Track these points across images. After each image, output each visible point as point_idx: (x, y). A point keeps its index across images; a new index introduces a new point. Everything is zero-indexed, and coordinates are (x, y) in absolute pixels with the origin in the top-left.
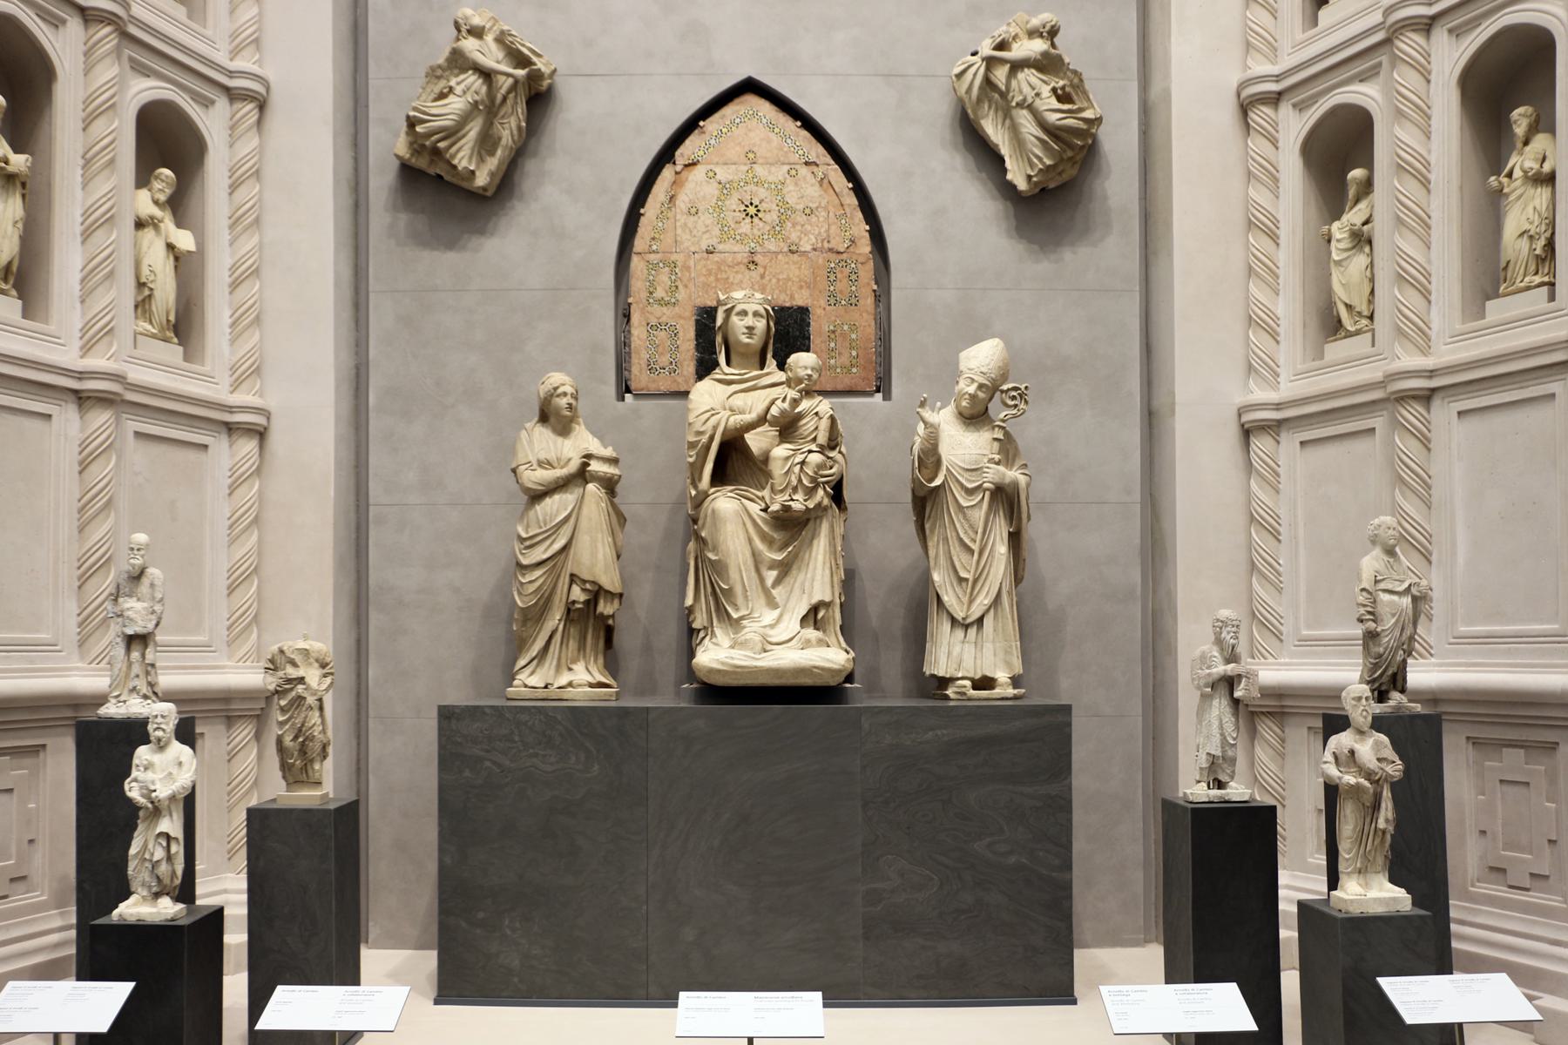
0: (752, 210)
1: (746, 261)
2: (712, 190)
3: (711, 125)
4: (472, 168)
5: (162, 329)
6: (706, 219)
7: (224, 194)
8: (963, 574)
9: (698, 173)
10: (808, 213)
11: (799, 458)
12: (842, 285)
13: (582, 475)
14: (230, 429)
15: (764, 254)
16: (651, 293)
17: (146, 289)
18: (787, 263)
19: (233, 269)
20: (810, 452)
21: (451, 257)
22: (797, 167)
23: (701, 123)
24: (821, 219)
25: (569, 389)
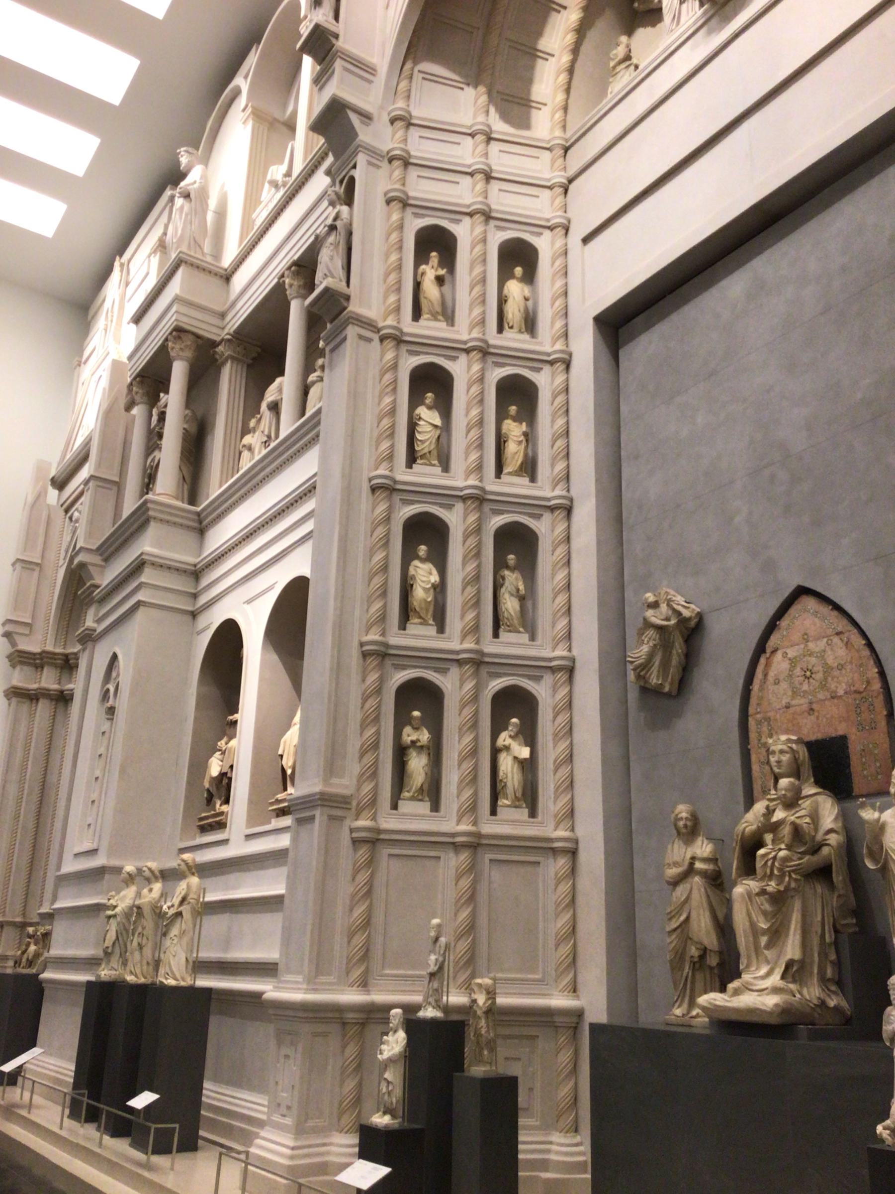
0: (808, 673)
1: (807, 709)
2: (785, 665)
3: (784, 623)
4: (660, 682)
5: (513, 801)
6: (784, 685)
7: (549, 724)
9: (779, 655)
10: (841, 667)
11: (773, 854)
12: (865, 715)
13: (690, 871)
14: (554, 851)
15: (817, 702)
16: (759, 740)
18: (831, 706)
19: (555, 761)
20: (780, 850)
22: (832, 638)
24: (848, 670)
25: (684, 815)
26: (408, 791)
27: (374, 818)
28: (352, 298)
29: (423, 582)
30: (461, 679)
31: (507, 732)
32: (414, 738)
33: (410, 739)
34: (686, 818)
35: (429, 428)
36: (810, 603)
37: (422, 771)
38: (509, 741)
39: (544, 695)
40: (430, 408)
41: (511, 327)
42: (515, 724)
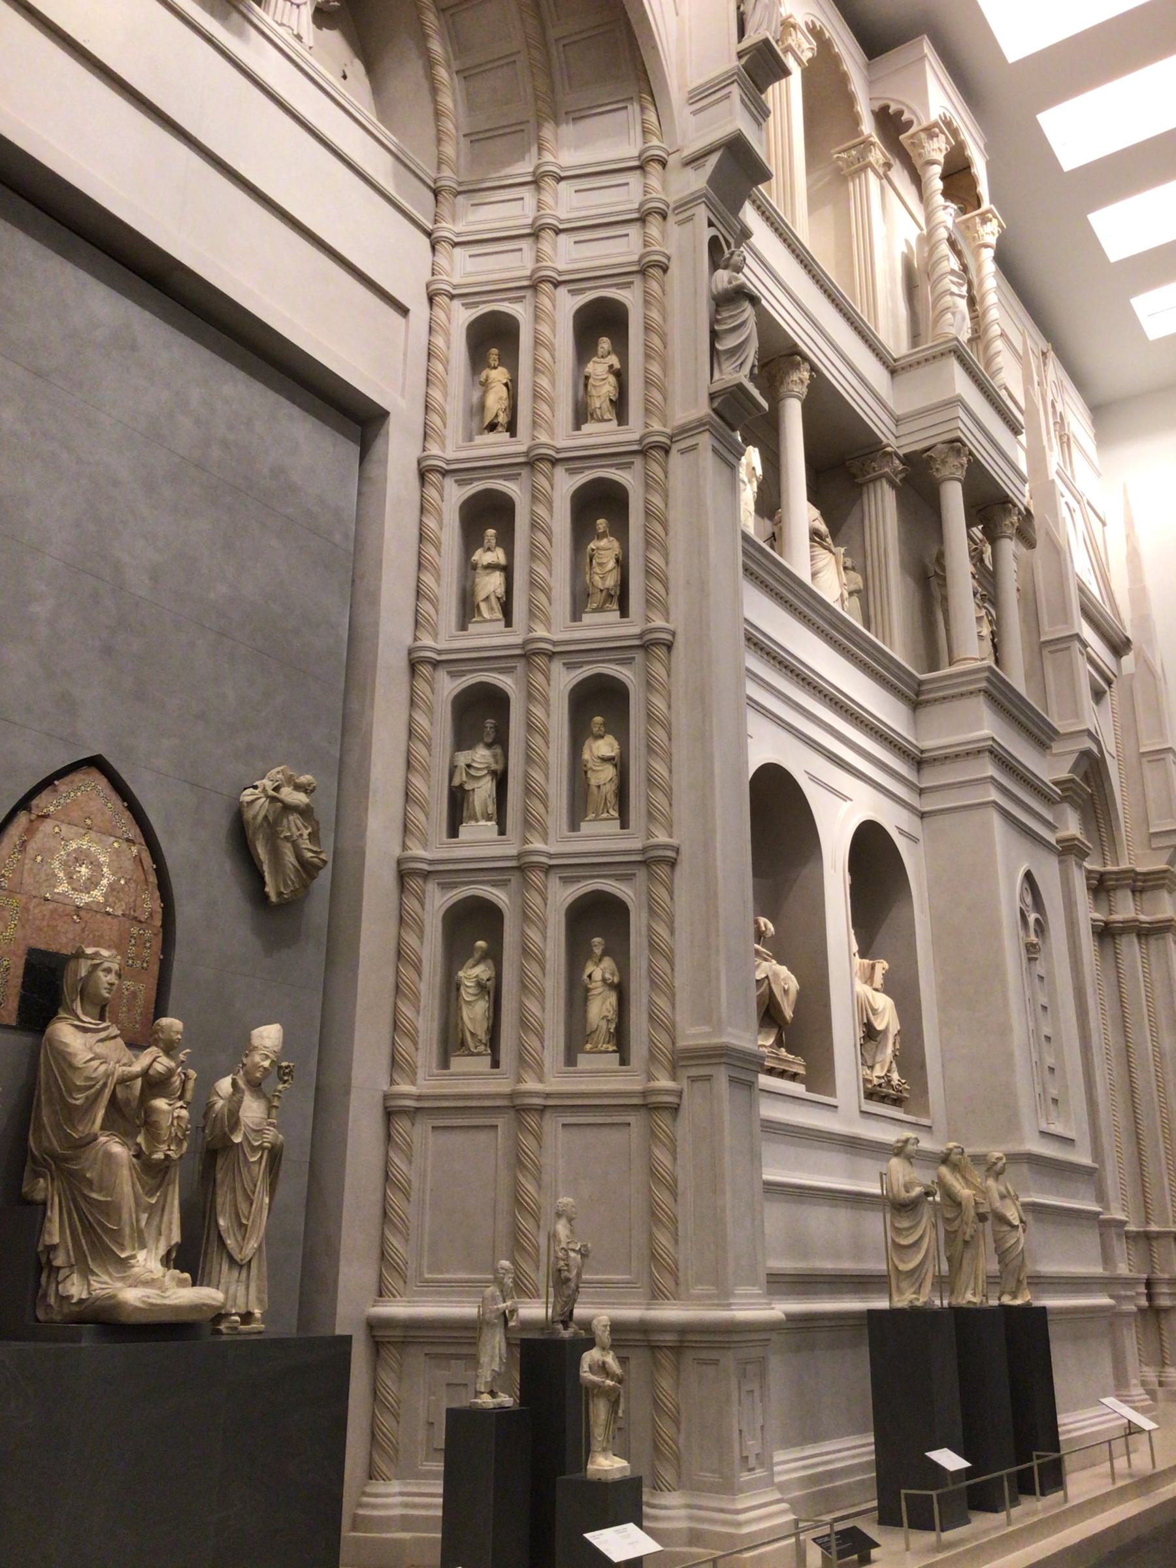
8: (244, 1221)
23: (56, 782)
36: (100, 783)
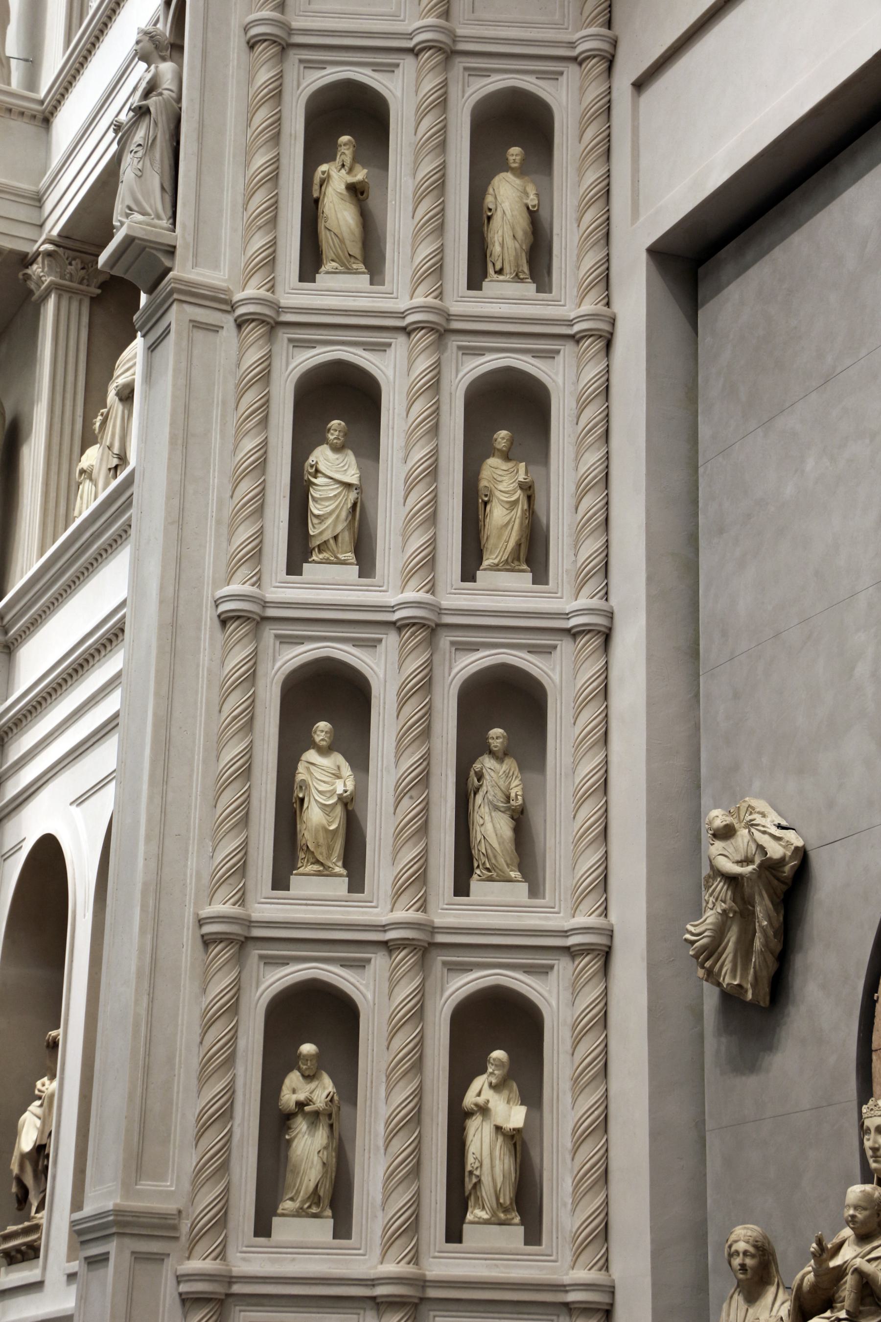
5: (494, 1214)
17: (474, 1177)
21: (752, 1081)
26: (292, 1199)
27: (221, 1254)
28: (178, 252)
29: (320, 792)
30: (390, 980)
31: (485, 1076)
32: (301, 1096)
33: (294, 1098)
34: (745, 1253)
35: (334, 490)
37: (316, 1158)
38: (488, 1094)
39: (554, 1003)
40: (337, 449)
41: (500, 272)
42: (499, 1064)
